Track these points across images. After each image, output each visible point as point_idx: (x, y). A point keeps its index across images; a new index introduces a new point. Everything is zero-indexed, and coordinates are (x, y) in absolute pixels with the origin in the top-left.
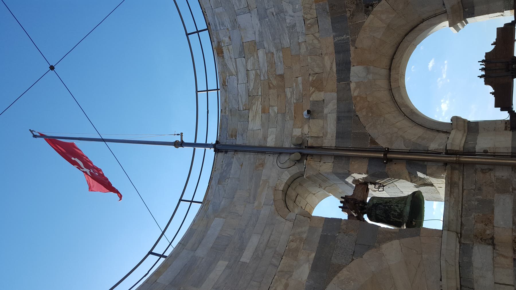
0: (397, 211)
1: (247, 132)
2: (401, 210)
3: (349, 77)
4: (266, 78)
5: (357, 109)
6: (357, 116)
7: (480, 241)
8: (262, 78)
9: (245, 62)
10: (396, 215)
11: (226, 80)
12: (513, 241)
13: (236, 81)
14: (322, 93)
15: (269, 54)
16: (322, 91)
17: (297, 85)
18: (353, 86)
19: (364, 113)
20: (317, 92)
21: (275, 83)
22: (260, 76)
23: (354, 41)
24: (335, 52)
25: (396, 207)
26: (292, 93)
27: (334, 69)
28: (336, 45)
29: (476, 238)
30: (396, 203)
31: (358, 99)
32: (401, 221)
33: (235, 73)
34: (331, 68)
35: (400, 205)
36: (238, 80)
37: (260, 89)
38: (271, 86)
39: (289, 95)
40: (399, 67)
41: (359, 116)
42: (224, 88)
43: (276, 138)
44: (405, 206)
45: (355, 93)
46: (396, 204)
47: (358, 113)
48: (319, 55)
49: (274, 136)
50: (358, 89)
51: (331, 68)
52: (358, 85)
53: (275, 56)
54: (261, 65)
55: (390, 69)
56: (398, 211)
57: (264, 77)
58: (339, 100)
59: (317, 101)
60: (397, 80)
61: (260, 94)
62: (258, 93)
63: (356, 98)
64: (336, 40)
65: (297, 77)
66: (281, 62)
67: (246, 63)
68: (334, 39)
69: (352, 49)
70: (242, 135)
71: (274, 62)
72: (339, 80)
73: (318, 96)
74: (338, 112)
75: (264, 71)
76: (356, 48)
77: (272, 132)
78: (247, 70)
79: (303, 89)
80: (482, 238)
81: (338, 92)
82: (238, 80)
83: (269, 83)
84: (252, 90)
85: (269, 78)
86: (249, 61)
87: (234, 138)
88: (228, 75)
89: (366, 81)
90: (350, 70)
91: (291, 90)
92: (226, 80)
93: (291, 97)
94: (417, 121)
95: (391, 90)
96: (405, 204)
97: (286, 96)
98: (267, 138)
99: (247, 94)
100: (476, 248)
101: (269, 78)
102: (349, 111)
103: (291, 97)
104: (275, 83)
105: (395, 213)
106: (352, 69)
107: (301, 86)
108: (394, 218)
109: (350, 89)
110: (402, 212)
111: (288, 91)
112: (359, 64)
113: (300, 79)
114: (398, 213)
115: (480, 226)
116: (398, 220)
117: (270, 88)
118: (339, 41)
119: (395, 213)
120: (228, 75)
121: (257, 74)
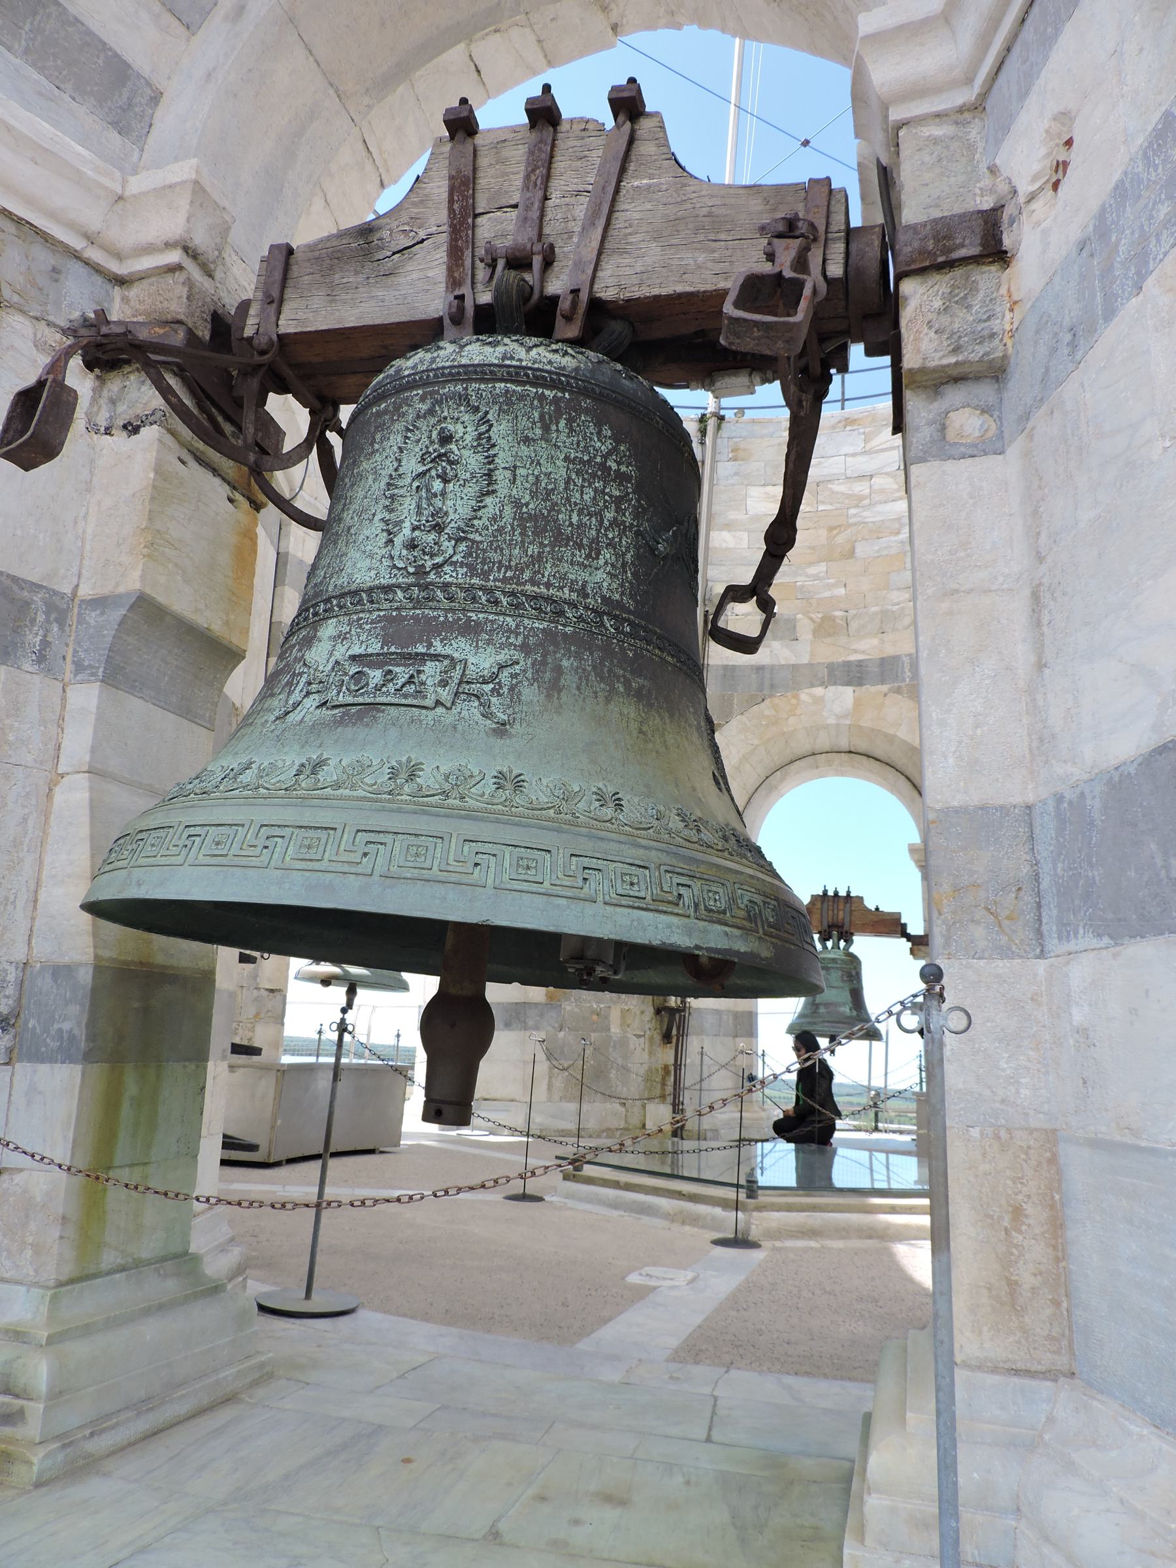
1: (742, 484)
3: (835, 684)
4: (852, 521)
5: (776, 700)
6: (763, 700)
8: (852, 511)
9: (889, 470)
11: (856, 427)
13: (851, 450)
14: (810, 636)
15: (897, 526)
16: (815, 637)
17: (830, 587)
18: (819, 691)
19: (767, 712)
20: (812, 627)
21: (840, 539)
22: (857, 506)
23: (898, 691)
24: (883, 659)
26: (816, 577)
27: (854, 657)
28: (896, 659)
31: (794, 701)
33: (868, 447)
34: (855, 651)
36: (854, 455)
37: (829, 507)
38: (835, 532)
39: (812, 570)
40: (852, 766)
41: (763, 704)
42: (840, 422)
43: (728, 549)
45: (804, 696)
47: (767, 701)
48: (881, 627)
49: (731, 544)
50: (810, 701)
51: (855, 651)
52: (819, 701)
53: (893, 538)
54: (879, 508)
55: (850, 752)
57: (855, 515)
58: (795, 668)
59: (795, 627)
60: (829, 763)
61: (820, 509)
62: (823, 502)
63: (797, 697)
64: (904, 659)
65: (845, 585)
66: (878, 551)
67: (886, 474)
68: (906, 655)
69: (885, 688)
70: (736, 474)
71: (880, 535)
72: (831, 667)
73: (805, 629)
74: (772, 668)
75: (865, 514)
76: (885, 695)
77: (741, 540)
78: (871, 476)
79: (821, 599)
81: (810, 665)
82: (854, 455)
83: (840, 526)
84: (831, 489)
85: (850, 525)
86: (890, 480)
87: (730, 456)
88: (867, 430)
89: (824, 714)
90: (847, 685)
91: (822, 575)
92: (856, 427)
93: (807, 576)
94: (756, 795)
95: (814, 754)
97: (811, 564)
98: (729, 531)
99: (821, 479)
101: (850, 525)
102: (772, 686)
103: (807, 576)
104: (840, 539)
106: (850, 689)
107: (827, 594)
109: (813, 686)
111: (822, 567)
112: (857, 703)
113: (842, 591)
117: (831, 529)
118: (903, 664)
120: (867, 430)
121: (861, 498)
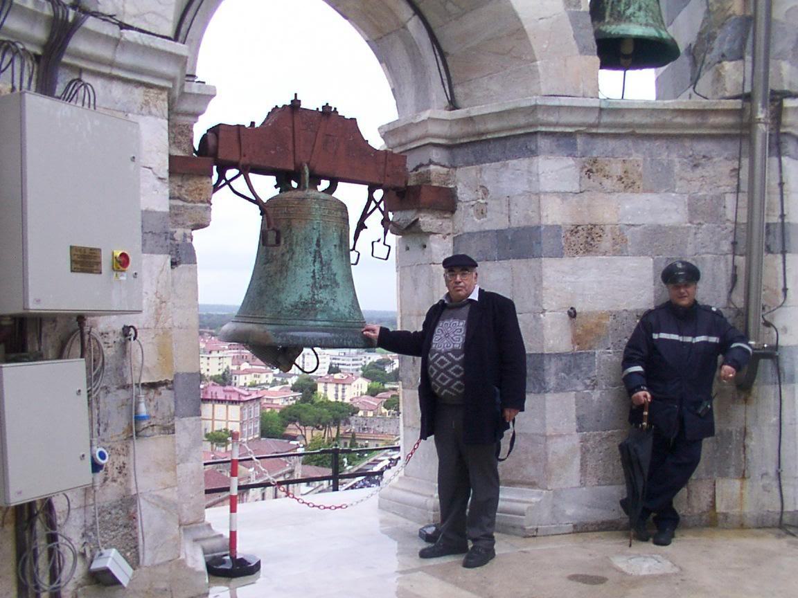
0: (628, 9)
2: (632, 18)
7: (586, 170)
10: (619, 9)
12: (595, 226)
25: (637, 6)
29: (592, 162)
30: (647, 6)
32: (607, 20)
35: (642, 13)
44: (641, 24)
46: (643, 5)
56: (628, 12)
80: (592, 172)
96: (647, 25)
100: (571, 161)
105: (622, 5)
108: (612, 6)
110: (629, 19)
114: (624, 12)
115: (616, 168)
116: (607, 14)
119: (622, 5)
